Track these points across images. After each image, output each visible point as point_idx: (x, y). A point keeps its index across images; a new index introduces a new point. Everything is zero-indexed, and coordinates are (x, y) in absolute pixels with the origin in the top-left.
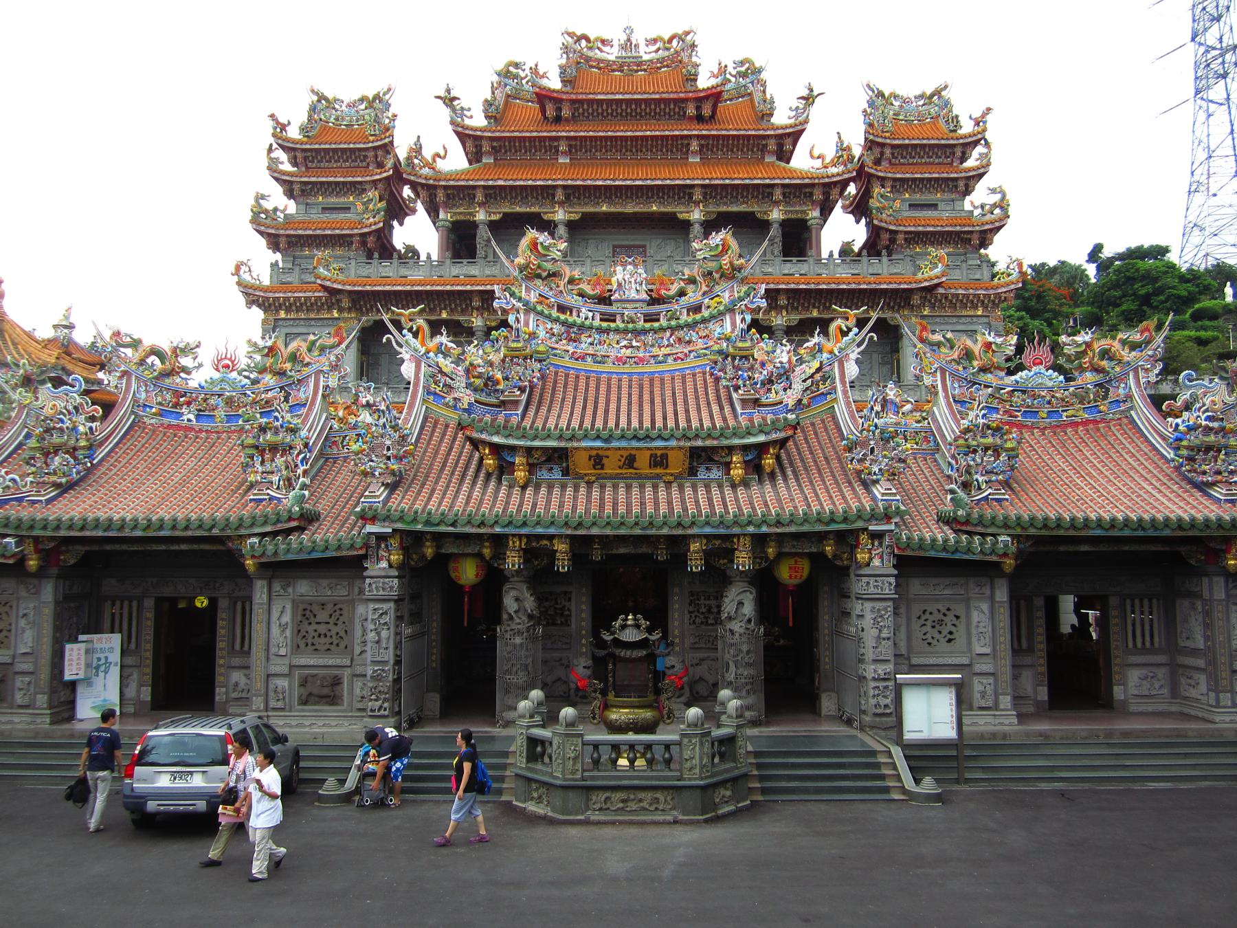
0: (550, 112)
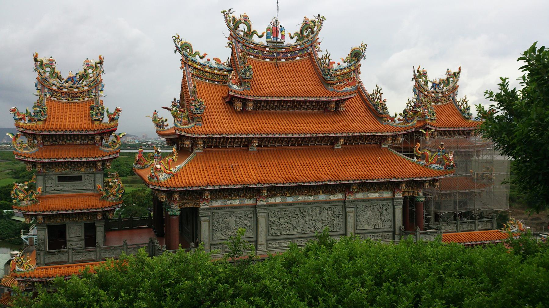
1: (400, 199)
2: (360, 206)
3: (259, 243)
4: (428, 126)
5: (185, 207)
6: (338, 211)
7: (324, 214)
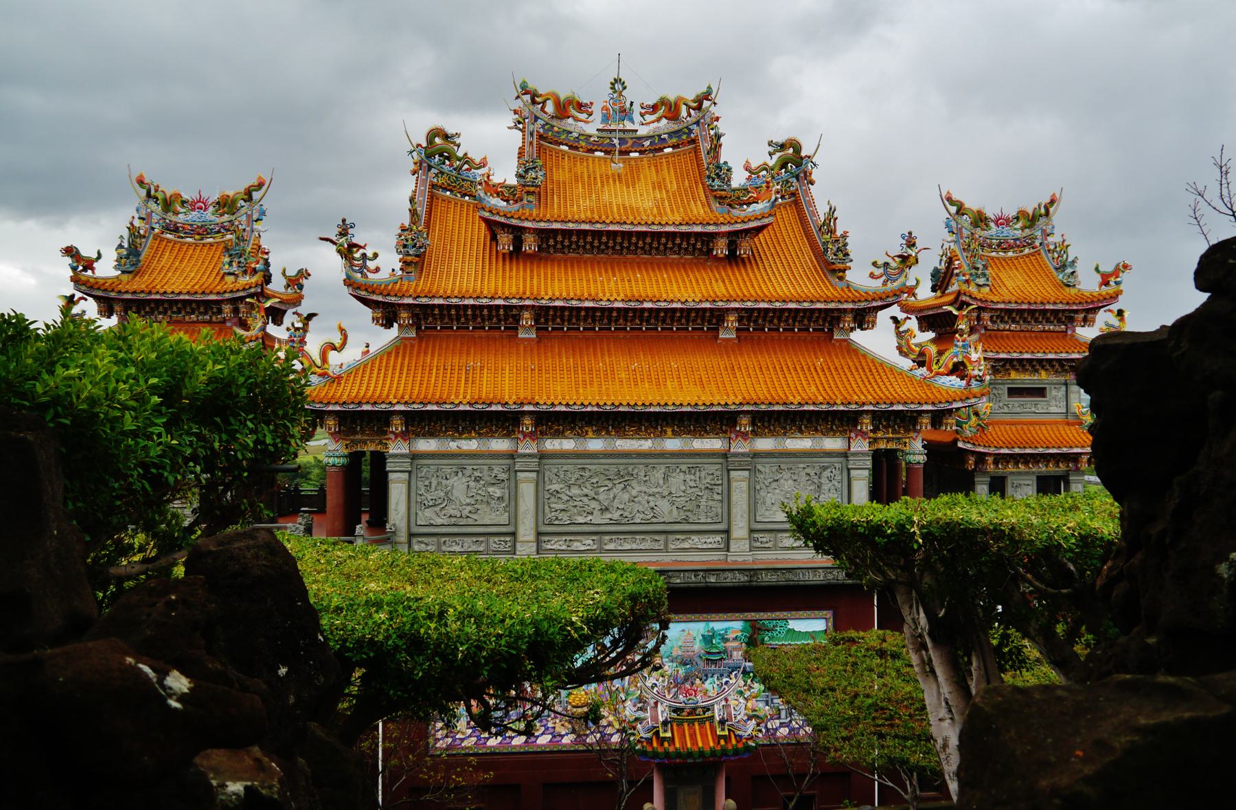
1: (863, 454)
2: (765, 468)
3: (520, 538)
4: (964, 298)
5: (359, 449)
6: (711, 477)
7: (677, 481)
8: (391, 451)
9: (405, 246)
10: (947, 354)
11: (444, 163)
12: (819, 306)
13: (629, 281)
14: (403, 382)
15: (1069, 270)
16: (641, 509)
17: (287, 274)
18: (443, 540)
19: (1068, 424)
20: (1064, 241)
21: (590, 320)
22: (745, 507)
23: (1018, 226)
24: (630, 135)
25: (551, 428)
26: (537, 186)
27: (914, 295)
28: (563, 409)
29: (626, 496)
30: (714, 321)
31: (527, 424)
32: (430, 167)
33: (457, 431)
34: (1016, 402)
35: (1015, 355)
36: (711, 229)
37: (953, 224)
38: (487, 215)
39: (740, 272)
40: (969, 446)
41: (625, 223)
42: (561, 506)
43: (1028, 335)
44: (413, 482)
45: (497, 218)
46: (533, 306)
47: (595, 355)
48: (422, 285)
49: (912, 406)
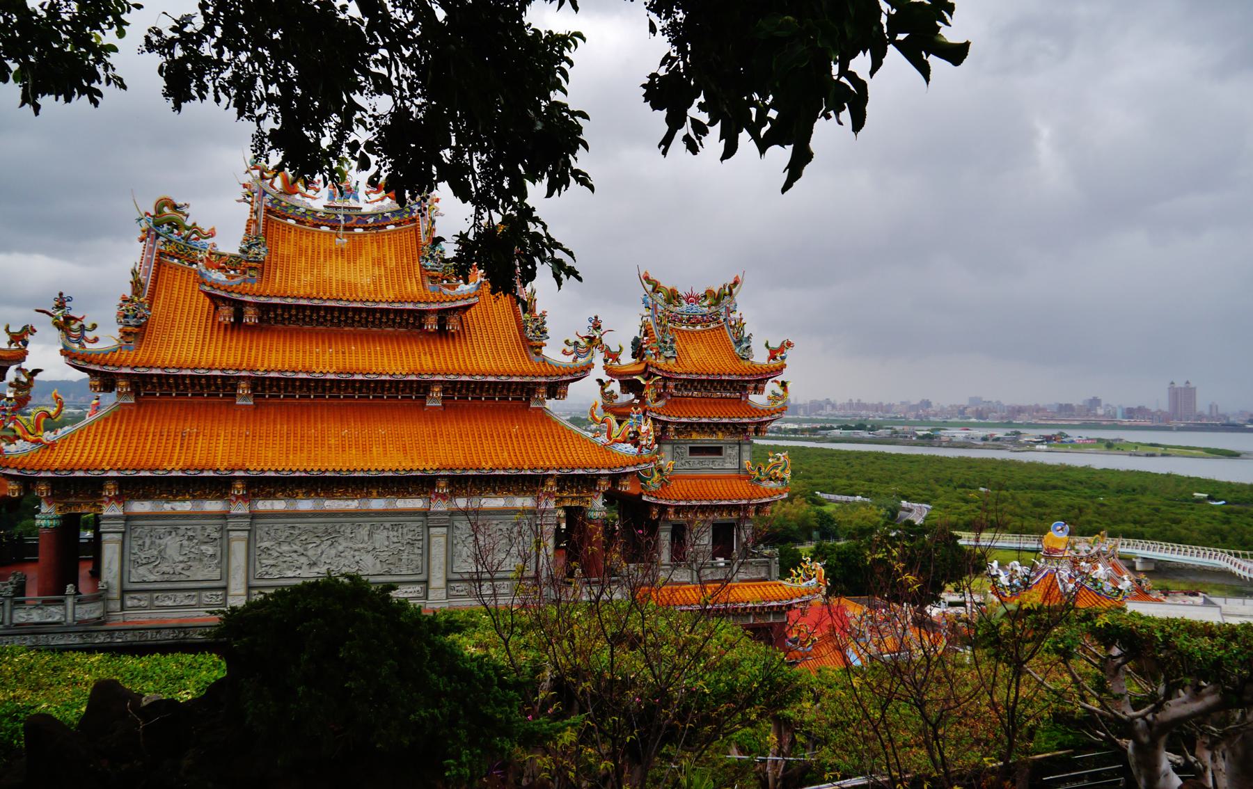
0: (226, 314)
3: (232, 592)
4: (651, 370)
5: (73, 511)
8: (105, 513)
9: (126, 316)
10: (624, 424)
11: (172, 232)
12: (516, 379)
13: (343, 353)
14: (118, 448)
15: (745, 345)
16: (347, 562)
17: (11, 330)
18: (156, 595)
19: (740, 478)
20: (741, 319)
21: (305, 389)
22: (443, 560)
23: (705, 304)
24: (356, 212)
25: (263, 490)
26: (259, 262)
27: (618, 360)
28: (273, 474)
29: (333, 552)
30: (421, 391)
31: (239, 489)
32: (158, 236)
33: (171, 493)
34: (696, 460)
35: (695, 420)
36: (422, 306)
37: (650, 300)
38: (208, 289)
39: (448, 346)
40: (652, 499)
41: (341, 299)
42: (272, 562)
43: (708, 401)
44: (127, 542)
45: (218, 292)
46: (250, 377)
47: (308, 421)
48: (142, 355)
49: (591, 471)
